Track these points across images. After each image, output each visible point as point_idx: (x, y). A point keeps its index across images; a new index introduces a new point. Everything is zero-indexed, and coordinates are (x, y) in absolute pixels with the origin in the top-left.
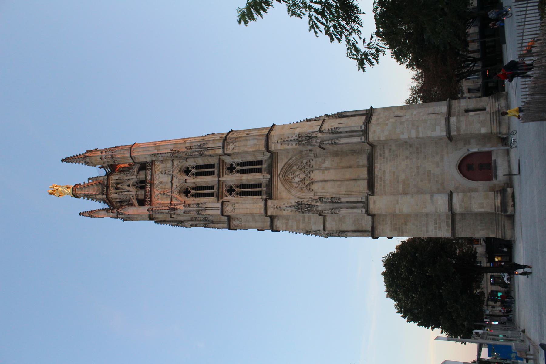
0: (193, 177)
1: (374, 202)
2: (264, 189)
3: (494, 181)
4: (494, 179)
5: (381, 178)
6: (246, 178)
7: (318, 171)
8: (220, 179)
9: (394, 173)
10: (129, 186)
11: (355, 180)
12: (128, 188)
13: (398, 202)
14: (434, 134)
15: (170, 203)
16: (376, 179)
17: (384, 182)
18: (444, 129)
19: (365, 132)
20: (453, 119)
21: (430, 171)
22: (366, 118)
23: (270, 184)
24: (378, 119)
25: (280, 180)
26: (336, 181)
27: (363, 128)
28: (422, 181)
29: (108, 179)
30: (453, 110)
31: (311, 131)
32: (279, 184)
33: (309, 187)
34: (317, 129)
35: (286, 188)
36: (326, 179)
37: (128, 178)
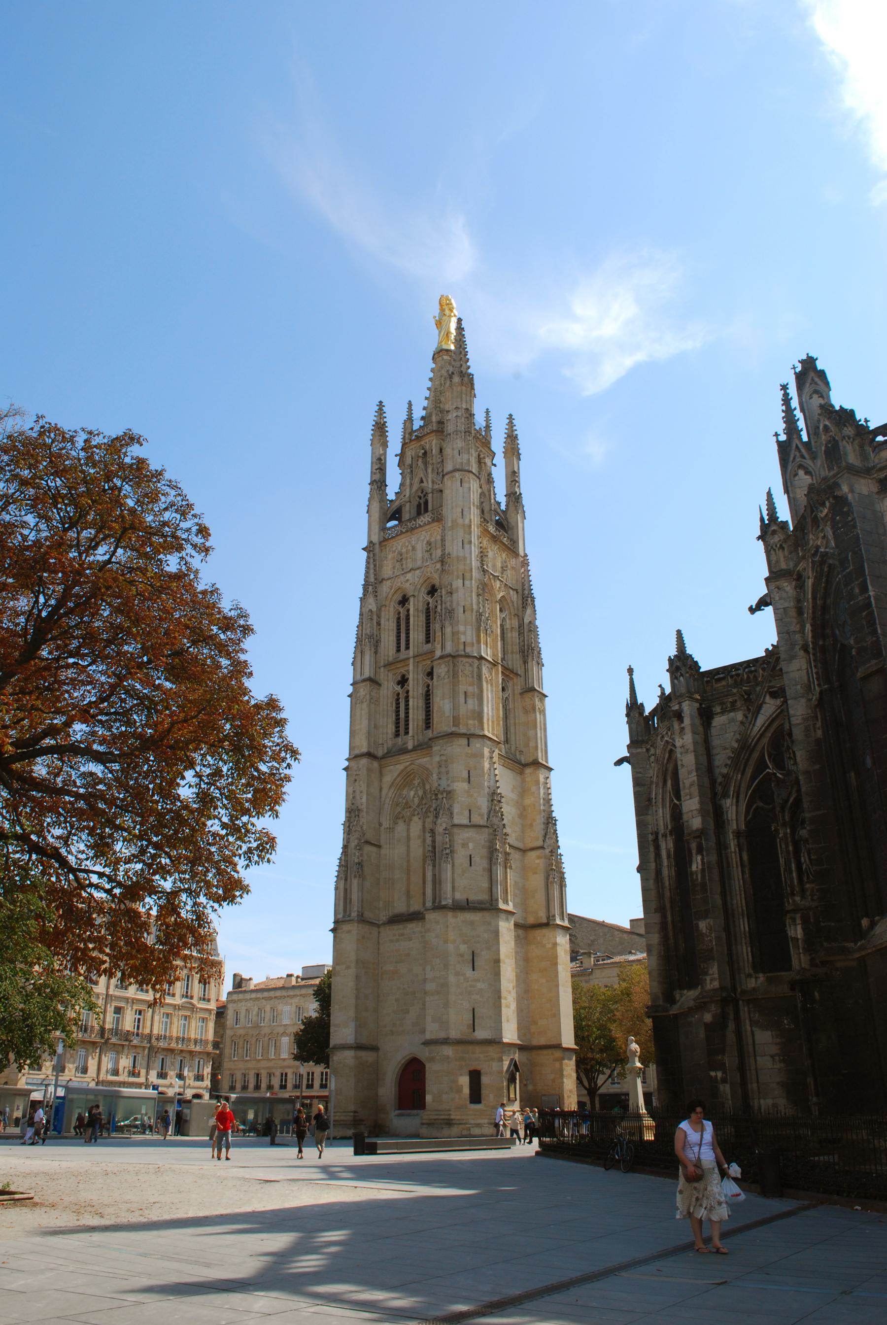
0: (422, 607)
1: (349, 932)
2: (399, 741)
3: (393, 1113)
4: (397, 1112)
5: (403, 935)
6: (416, 704)
7: (421, 827)
8: (411, 660)
9: (408, 955)
10: (422, 481)
11: (408, 892)
12: (416, 480)
13: (348, 968)
14: (429, 1019)
15: (383, 580)
16: (401, 926)
17: (398, 940)
18: (433, 1037)
19: (438, 907)
20: (448, 1051)
21: (408, 1012)
22: (480, 902)
23: (404, 751)
24: (472, 923)
25: (406, 768)
26: (408, 861)
27: (443, 903)
28: (397, 1000)
29: (433, 432)
30: (478, 1049)
31: (456, 809)
32: (400, 767)
33: (396, 818)
34: (456, 821)
35: (395, 780)
36: (412, 842)
37: (430, 475)
